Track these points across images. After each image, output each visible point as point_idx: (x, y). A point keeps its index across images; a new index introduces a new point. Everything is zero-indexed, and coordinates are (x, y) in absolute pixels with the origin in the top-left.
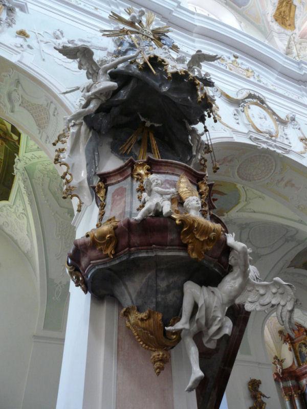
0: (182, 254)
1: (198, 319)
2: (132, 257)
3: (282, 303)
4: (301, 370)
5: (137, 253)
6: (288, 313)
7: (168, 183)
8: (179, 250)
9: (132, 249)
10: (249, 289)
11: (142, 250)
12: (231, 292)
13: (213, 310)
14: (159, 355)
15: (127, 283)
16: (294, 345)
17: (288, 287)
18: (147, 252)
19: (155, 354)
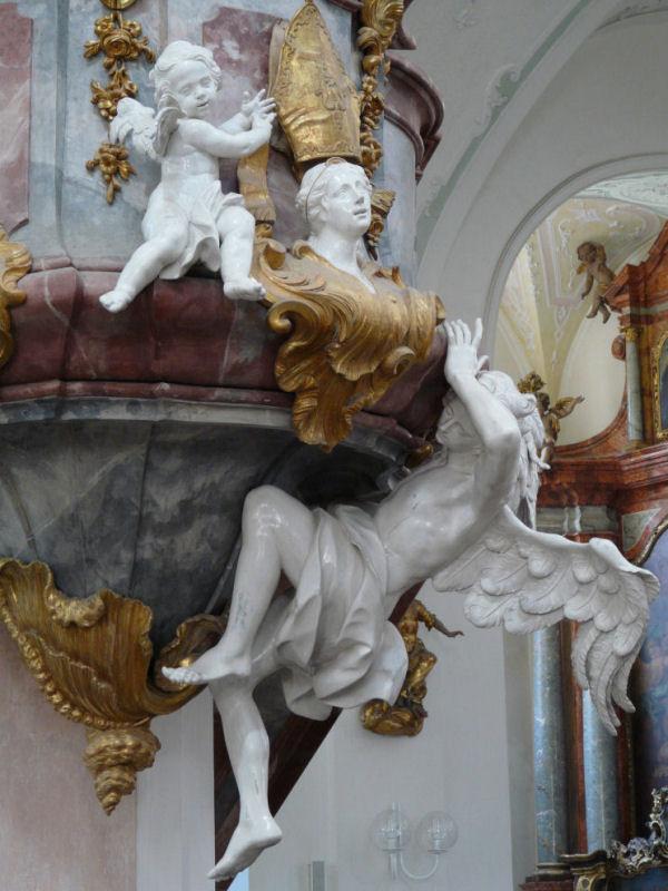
0: (268, 419)
1: (283, 645)
2: (69, 416)
3: (602, 622)
4: (651, 463)
5: (91, 403)
6: (613, 660)
7: (234, 30)
8: (259, 405)
9: (77, 386)
10: (494, 543)
11: (118, 402)
12: (424, 552)
13: (347, 621)
14: (120, 748)
15: (15, 471)
16: (648, 329)
17: (635, 584)
18: (133, 405)
19: (108, 741)
